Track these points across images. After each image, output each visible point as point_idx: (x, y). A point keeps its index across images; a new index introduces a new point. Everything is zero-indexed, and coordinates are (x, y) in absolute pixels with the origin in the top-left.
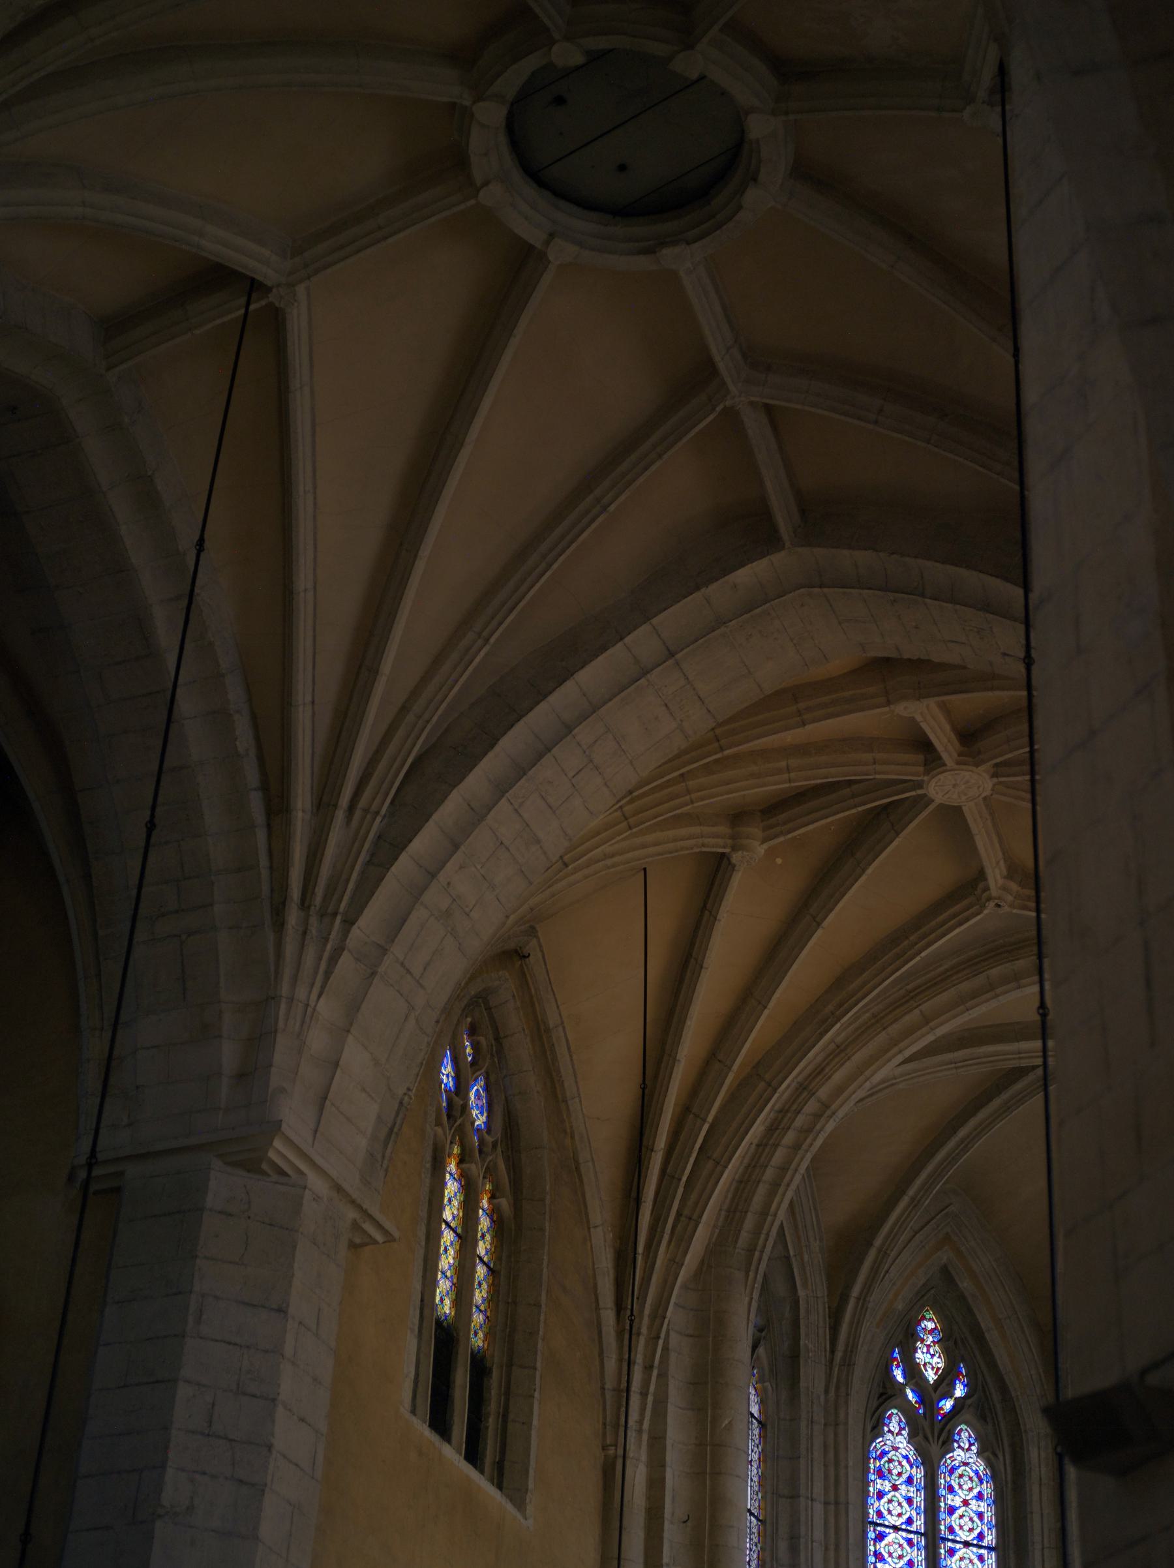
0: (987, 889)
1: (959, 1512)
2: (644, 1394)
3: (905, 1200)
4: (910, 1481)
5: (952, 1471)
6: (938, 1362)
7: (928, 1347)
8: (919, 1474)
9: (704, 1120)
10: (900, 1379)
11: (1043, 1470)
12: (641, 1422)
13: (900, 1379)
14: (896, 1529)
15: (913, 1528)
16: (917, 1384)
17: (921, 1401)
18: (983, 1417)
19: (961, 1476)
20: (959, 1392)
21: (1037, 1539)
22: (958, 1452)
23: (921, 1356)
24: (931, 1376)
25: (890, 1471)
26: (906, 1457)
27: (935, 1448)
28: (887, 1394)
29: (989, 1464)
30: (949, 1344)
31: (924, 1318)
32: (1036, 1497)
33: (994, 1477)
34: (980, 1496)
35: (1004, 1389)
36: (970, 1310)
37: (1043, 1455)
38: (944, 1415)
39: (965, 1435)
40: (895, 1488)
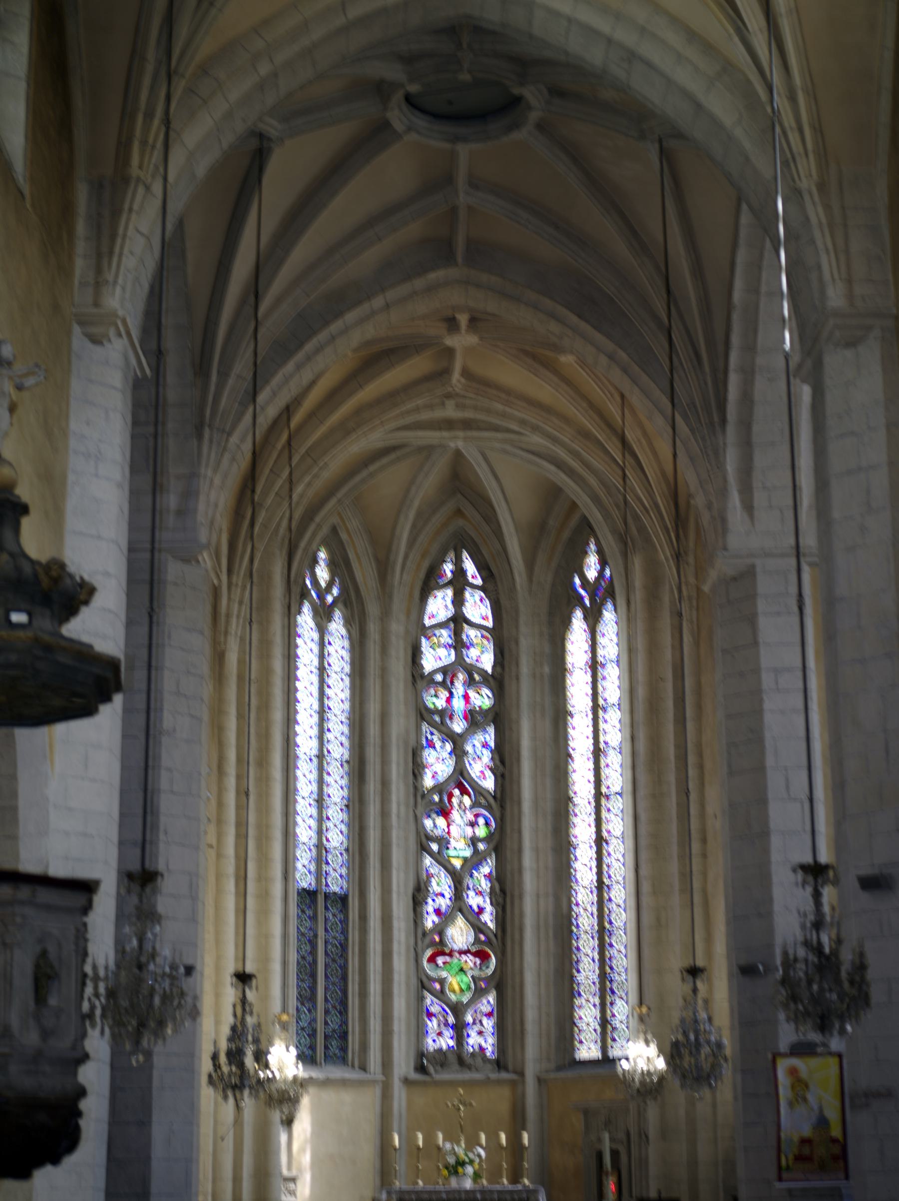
17: (318, 597)
18: (345, 605)
20: (335, 591)
24: (323, 584)
28: (304, 594)
29: (348, 631)
30: (332, 566)
36: (344, 549)
39: (337, 614)
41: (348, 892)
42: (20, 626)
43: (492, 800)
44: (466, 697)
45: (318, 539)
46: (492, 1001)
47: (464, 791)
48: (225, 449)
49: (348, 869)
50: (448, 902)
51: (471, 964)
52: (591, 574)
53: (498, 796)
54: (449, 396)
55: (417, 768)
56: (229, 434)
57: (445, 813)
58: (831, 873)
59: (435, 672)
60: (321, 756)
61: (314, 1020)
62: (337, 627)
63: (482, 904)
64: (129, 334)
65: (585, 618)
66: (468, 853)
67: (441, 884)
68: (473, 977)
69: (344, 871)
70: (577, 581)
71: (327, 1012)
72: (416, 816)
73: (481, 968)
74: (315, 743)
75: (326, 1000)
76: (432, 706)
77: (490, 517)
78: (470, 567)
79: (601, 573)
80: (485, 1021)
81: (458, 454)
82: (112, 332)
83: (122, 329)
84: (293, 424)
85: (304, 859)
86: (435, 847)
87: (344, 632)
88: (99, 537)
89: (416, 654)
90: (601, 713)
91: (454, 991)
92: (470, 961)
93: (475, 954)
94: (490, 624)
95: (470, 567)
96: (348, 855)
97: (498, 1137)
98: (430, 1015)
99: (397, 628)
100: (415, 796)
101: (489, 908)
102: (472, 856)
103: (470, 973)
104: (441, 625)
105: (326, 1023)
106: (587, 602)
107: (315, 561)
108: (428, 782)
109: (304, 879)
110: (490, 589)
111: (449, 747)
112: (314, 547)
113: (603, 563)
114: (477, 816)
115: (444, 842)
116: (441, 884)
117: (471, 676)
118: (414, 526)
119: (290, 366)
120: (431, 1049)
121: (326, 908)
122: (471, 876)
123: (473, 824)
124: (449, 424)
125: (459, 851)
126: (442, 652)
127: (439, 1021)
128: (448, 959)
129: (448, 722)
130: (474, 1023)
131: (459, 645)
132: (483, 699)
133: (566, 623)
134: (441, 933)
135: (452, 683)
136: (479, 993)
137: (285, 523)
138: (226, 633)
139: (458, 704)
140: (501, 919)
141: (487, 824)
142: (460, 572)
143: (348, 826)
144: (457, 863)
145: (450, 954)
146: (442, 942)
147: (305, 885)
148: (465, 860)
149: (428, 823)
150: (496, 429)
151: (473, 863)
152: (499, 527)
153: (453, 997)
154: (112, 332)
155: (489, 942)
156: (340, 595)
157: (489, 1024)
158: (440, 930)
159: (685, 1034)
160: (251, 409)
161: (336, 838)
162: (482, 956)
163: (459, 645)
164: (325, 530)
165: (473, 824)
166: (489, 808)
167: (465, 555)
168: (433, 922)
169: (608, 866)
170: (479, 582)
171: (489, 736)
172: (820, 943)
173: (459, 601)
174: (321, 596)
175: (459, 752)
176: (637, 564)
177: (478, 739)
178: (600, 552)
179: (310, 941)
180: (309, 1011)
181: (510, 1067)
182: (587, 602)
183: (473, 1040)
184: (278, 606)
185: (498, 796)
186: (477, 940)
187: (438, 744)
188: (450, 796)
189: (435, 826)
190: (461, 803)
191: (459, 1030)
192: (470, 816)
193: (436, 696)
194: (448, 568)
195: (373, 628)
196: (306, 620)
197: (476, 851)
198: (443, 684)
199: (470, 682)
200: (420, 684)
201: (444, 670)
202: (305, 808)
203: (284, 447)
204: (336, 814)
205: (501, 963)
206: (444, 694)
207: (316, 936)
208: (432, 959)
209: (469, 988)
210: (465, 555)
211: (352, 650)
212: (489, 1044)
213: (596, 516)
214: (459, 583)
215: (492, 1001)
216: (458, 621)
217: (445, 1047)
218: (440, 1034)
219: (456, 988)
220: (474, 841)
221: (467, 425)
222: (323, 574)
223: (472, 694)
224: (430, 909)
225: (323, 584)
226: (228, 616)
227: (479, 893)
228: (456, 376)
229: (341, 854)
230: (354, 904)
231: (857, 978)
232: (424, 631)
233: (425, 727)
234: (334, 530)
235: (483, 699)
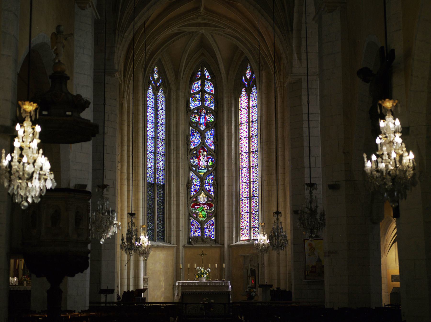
0: (200, 11)
1: (160, 104)
2: (127, 92)
3: (160, 50)
4: (152, 98)
5: (159, 96)
6: (157, 76)
7: (156, 73)
8: (154, 97)
9: (141, 44)
10: (151, 80)
11: (174, 97)
12: (127, 97)
13: (151, 80)
14: (150, 107)
15: (153, 107)
16: (154, 81)
18: (164, 86)
19: (160, 97)
21: (173, 109)
22: (160, 93)
23: (154, 75)
24: (156, 79)
25: (149, 97)
26: (152, 94)
27: (157, 93)
28: (150, 83)
29: (165, 95)
30: (159, 72)
31: (155, 68)
32: (173, 102)
33: (165, 97)
34: (163, 101)
35: (168, 81)
37: (174, 94)
38: (158, 86)
39: (161, 90)
40: (150, 100)
41: (165, 184)
42: (69, 116)
43: (213, 153)
44: (205, 118)
45: (154, 64)
46: (213, 220)
47: (204, 151)
48: (123, 37)
49: (165, 176)
50: (199, 187)
51: (206, 208)
52: (248, 76)
53: (216, 151)
54: (200, 16)
55: (188, 142)
56: (125, 33)
57: (198, 158)
58: (315, 186)
59: (194, 109)
60: (156, 138)
61: (153, 227)
62: (161, 94)
63: (210, 188)
64: (93, 6)
65: (246, 91)
66: (205, 171)
67: (196, 181)
68: (206, 212)
69: (163, 177)
70: (244, 79)
71: (158, 224)
72: (188, 159)
73: (209, 209)
74: (153, 134)
75: (157, 220)
76: (193, 121)
77: (214, 56)
78: (207, 73)
79: (252, 75)
80: (211, 226)
81: (203, 34)
82: (88, 5)
83: (91, 5)
84: (145, 26)
85: (150, 172)
86: (194, 169)
87: (163, 95)
88: (85, 74)
89: (188, 104)
90: (251, 124)
91: (200, 217)
92: (206, 207)
93: (208, 205)
94: (213, 93)
95: (207, 73)
96: (165, 171)
97: (215, 265)
98: (193, 225)
99: (181, 94)
100: (188, 151)
101: (212, 189)
102: (207, 172)
103: (206, 211)
104: (197, 93)
105: (157, 228)
106: (247, 86)
107: (153, 72)
108: (192, 147)
109: (150, 180)
110: (213, 81)
111: (199, 135)
112: (153, 66)
113: (252, 72)
114: (209, 158)
115: (197, 167)
116: (196, 181)
117: (207, 111)
118: (187, 59)
119: (145, 8)
120: (193, 236)
121: (157, 189)
122: (207, 179)
123: (207, 161)
124: (199, 25)
125: (203, 171)
126: (197, 102)
127: (195, 227)
128: (198, 206)
129: (199, 126)
130: (207, 228)
131: (203, 100)
132: (211, 119)
133: (240, 94)
134: (196, 198)
135: (200, 113)
136: (209, 218)
137: (143, 59)
138: (123, 98)
139: (202, 120)
140: (216, 193)
141: (212, 161)
142: (203, 75)
143: (165, 161)
144: (202, 174)
145: (199, 205)
146: (196, 201)
147: (150, 181)
148: (205, 173)
149: (192, 161)
150: (216, 27)
151: (207, 174)
152: (217, 59)
153: (200, 219)
154: (88, 5)
155: (212, 201)
156: (161, 83)
157: (212, 228)
158: (196, 197)
159: (274, 233)
160: (133, 23)
161: (160, 166)
162: (210, 205)
163: (203, 100)
164: (157, 61)
165: (207, 161)
166: (212, 155)
167: (205, 69)
168: (193, 194)
169: (253, 176)
170: (210, 78)
171: (213, 131)
172: (311, 207)
173: (203, 85)
174: (156, 82)
175: (202, 137)
176: (264, 73)
177: (209, 133)
178: (251, 68)
179: (152, 200)
180: (152, 223)
181: (219, 242)
182: (247, 86)
183: (207, 233)
184: (141, 88)
185: (216, 151)
186: (208, 200)
187: (195, 134)
188: (200, 152)
189: (194, 161)
190: (203, 154)
191: (202, 230)
192: (206, 158)
193: (195, 117)
194: (199, 74)
195: (173, 94)
196: (150, 91)
197: (208, 171)
198: (197, 113)
199: (206, 113)
200: (190, 114)
201: (198, 109)
202: (150, 156)
203: (143, 33)
204: (160, 157)
205: (216, 208)
206: (197, 117)
207: (154, 199)
208: (193, 207)
209: (206, 216)
210: (205, 69)
211: (166, 102)
212: (212, 235)
213: (250, 56)
214: (203, 79)
215: (213, 220)
216: (202, 92)
217: (197, 235)
218: (196, 231)
219: (201, 216)
220: (207, 167)
221: (206, 25)
222: (156, 76)
223: (207, 117)
224: (192, 190)
225: (156, 79)
226: (124, 92)
227: (209, 184)
228: (202, 9)
229: (162, 171)
230: (167, 188)
231: (322, 218)
232: (191, 95)
233: (191, 128)
234: (160, 60)
235: (211, 119)
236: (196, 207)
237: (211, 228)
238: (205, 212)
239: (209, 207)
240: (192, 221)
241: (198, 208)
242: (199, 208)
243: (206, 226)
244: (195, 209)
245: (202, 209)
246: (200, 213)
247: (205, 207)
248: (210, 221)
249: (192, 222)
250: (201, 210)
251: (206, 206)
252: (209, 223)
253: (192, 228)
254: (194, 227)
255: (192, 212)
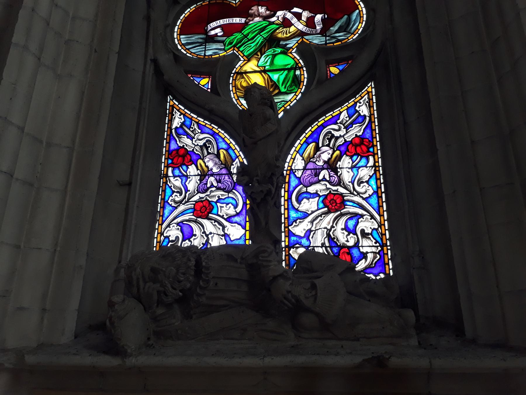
46: (364, 110)
73: (323, 32)
127: (204, 175)
128: (237, 20)
209: (296, 81)
215: (364, 110)
236: (214, 24)
237: (347, 176)
238: (286, 51)
239: (318, 17)
240: (177, 122)
241: (228, 30)
242: (240, 28)
243: (299, 164)
244: (213, 39)
245: (265, 34)
246: (252, 65)
247: (286, 23)
248: (334, 120)
249: (181, 131)
250: (259, 39)
251: (298, 16)
252: (331, 137)
253: (177, 183)
254: (192, 170)
255: (178, 57)
